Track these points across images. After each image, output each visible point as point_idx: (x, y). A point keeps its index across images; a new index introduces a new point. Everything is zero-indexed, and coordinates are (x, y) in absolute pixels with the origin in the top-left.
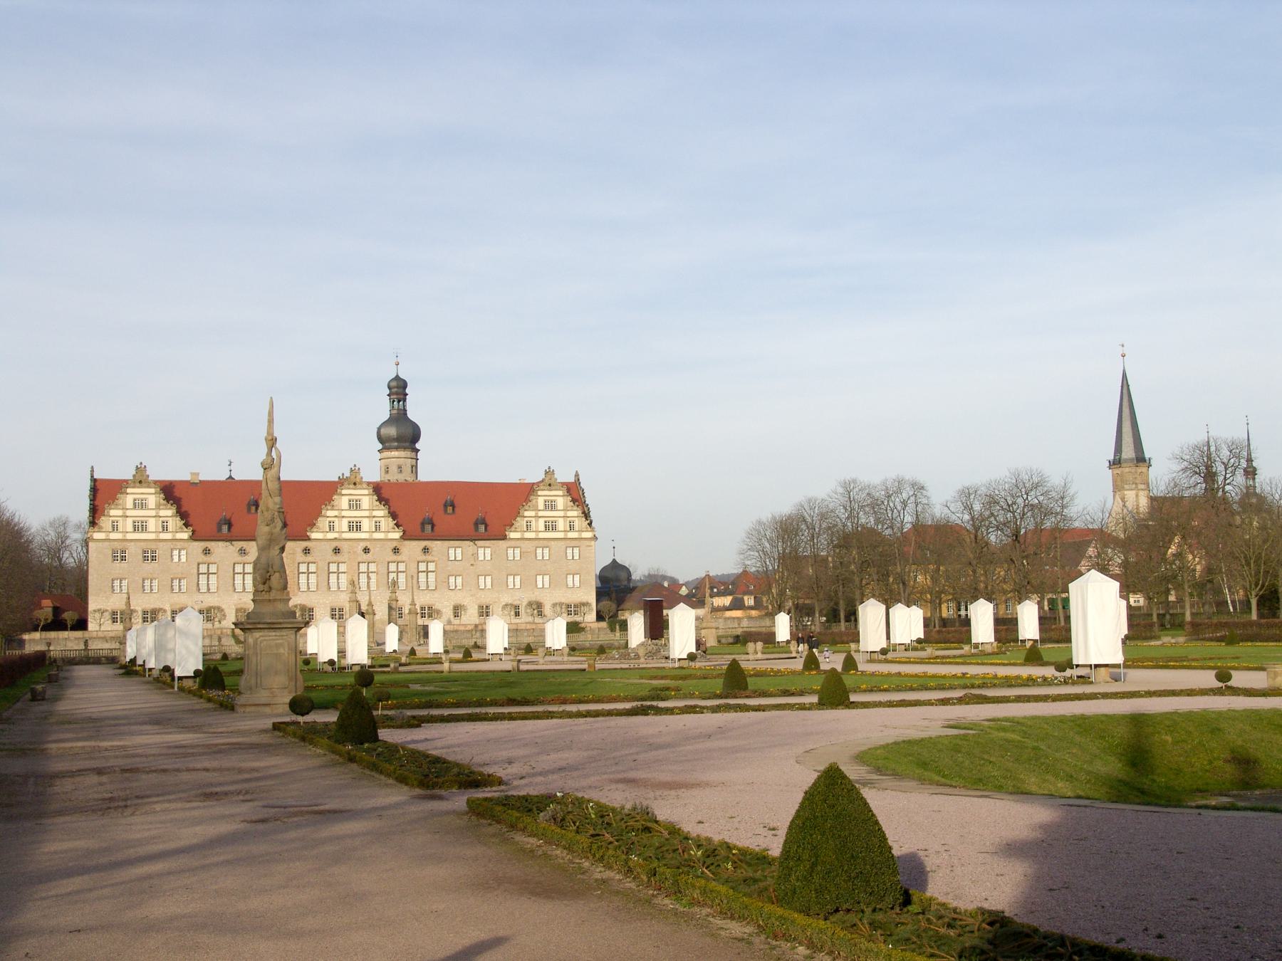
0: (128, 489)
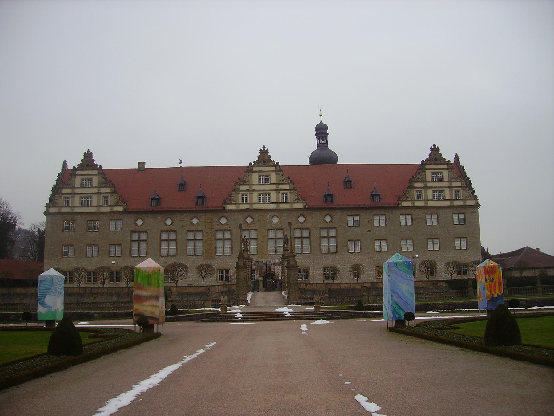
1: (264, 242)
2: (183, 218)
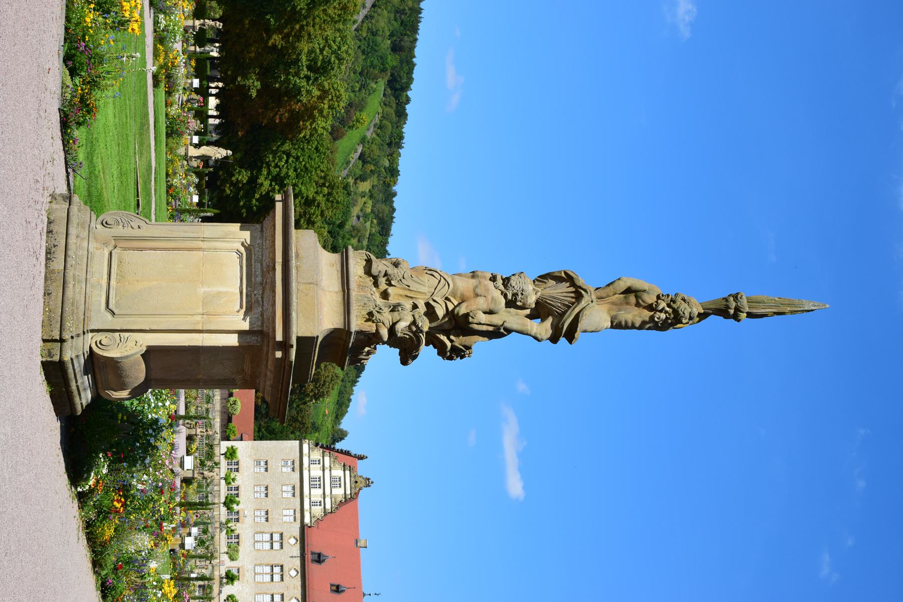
0: (349, 472)
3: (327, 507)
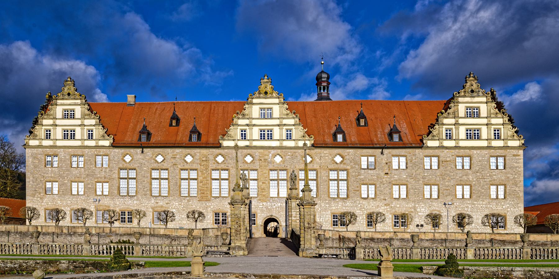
1: (265, 183)
2: (175, 155)
3: (94, 123)
